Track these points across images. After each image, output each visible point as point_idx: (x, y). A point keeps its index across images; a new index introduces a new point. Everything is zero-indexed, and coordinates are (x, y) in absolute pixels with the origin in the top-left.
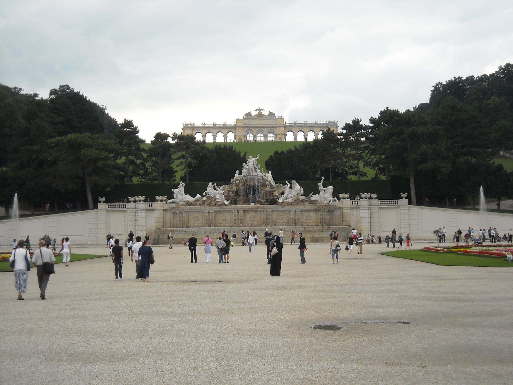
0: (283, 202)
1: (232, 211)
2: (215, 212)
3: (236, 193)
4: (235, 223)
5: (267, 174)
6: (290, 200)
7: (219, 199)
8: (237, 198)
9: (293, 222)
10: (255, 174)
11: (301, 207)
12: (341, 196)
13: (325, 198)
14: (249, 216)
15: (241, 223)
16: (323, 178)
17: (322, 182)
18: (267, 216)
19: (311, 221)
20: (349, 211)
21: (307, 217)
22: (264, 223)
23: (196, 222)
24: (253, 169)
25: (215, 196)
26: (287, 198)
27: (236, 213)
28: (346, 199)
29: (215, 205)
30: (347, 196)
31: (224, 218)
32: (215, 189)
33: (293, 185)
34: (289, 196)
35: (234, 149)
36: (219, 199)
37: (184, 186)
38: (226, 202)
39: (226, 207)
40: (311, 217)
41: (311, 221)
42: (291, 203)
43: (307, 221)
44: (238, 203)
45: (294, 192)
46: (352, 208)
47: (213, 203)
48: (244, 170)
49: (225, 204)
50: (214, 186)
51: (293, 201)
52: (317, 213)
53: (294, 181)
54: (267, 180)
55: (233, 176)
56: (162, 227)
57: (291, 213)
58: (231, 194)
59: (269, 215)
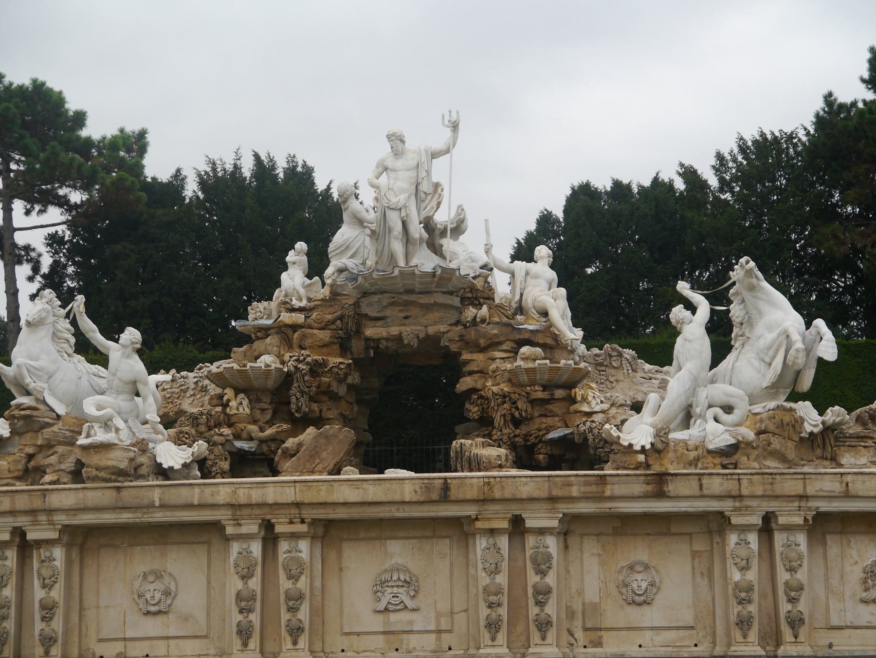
0: (657, 450)
1: (216, 527)
2: (85, 539)
3: (275, 397)
4: (245, 633)
6: (715, 433)
7: (106, 424)
9: (744, 623)
10: (425, 262)
11: (823, 483)
15: (295, 632)
18: (517, 576)
22: (493, 626)
24: (417, 230)
25: (76, 403)
26: (687, 417)
27: (256, 548)
29: (77, 475)
31: (153, 591)
32: (84, 347)
33: (736, 312)
34: (704, 395)
35: (320, 185)
36: (106, 424)
38: (172, 455)
39: (154, 491)
42: (730, 453)
45: (749, 368)
47: (59, 461)
48: (344, 234)
49: (164, 473)
50: (74, 323)
51: (749, 434)
53: (744, 269)
54: (520, 309)
55: (267, 285)
57: (733, 538)
58: (239, 406)
59: (542, 565)
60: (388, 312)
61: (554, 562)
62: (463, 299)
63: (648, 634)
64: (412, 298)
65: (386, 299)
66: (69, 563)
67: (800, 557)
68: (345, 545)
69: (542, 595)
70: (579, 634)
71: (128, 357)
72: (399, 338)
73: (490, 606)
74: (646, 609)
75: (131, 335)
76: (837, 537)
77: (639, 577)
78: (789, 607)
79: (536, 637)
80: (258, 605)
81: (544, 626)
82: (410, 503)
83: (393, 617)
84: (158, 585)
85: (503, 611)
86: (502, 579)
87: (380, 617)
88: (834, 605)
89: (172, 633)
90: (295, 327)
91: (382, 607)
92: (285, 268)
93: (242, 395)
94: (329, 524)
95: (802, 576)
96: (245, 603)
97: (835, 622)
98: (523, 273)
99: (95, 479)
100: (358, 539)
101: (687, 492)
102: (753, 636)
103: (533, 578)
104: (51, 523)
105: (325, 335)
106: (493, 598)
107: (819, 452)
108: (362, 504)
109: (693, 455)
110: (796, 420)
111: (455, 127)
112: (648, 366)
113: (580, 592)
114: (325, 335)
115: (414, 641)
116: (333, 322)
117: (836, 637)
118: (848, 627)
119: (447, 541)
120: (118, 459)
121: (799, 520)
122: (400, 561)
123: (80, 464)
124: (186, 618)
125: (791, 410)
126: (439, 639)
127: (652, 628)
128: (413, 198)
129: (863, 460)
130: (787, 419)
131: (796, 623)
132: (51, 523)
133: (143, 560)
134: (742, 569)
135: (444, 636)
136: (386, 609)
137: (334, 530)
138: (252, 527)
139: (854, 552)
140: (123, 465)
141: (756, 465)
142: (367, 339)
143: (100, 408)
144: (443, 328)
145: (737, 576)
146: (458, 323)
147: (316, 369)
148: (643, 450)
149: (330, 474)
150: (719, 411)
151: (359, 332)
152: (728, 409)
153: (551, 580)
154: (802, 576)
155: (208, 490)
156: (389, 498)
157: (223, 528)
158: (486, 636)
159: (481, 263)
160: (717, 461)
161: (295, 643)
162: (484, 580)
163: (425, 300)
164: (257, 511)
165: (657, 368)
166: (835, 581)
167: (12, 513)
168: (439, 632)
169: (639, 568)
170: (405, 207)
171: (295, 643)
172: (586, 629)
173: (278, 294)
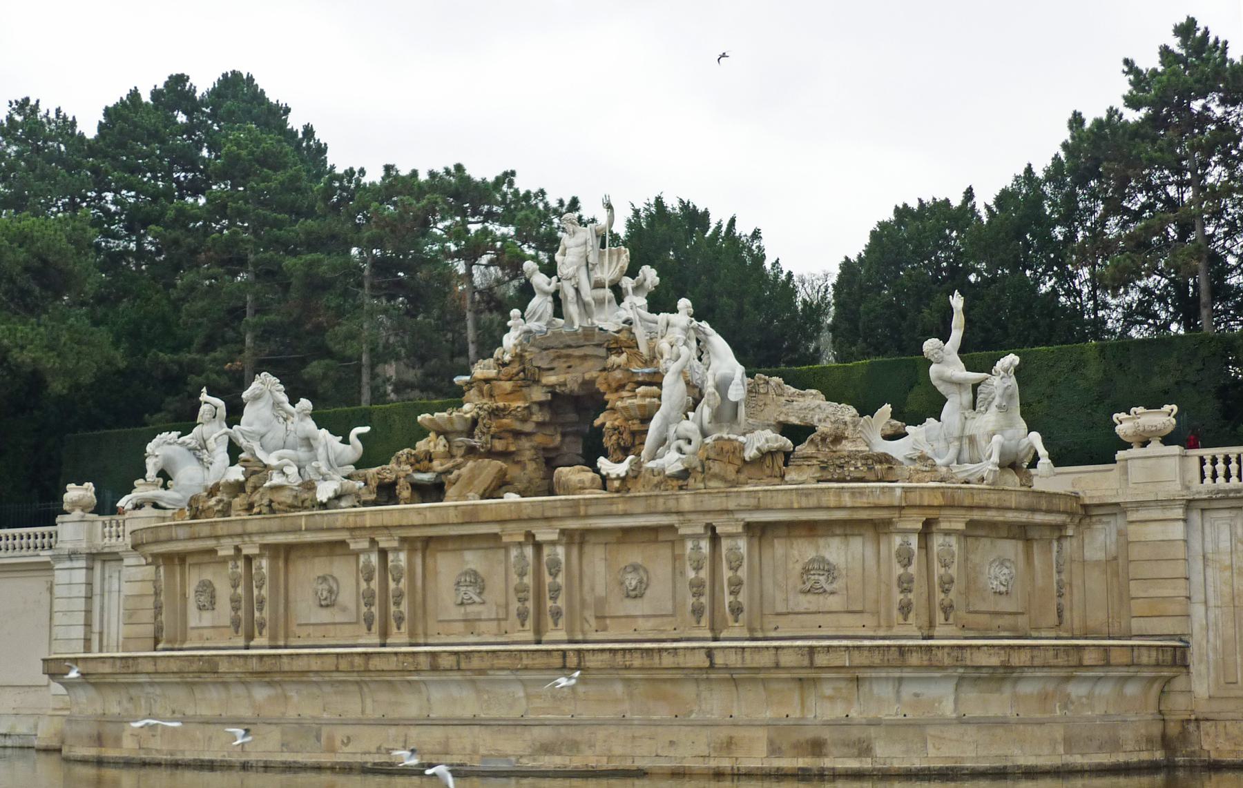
1: (343, 543)
2: (284, 553)
5: (663, 317)
6: (671, 461)
8: (449, 472)
9: (697, 612)
12: (1125, 424)
13: (972, 440)
14: (447, 568)
16: (957, 301)
17: (957, 335)
19: (834, 602)
20: (1177, 531)
21: (806, 571)
23: (207, 619)
28: (1156, 448)
30: (1164, 418)
37: (222, 411)
40: (830, 571)
41: (834, 602)
43: (805, 602)
44: (451, 491)
46: (1189, 504)
49: (323, 506)
52: (884, 540)
56: (151, 643)
57: (689, 545)
60: (555, 364)
61: (563, 566)
62: (609, 349)
63: (640, 621)
64: (570, 351)
65: (552, 353)
66: (273, 570)
67: (740, 559)
68: (440, 556)
69: (556, 591)
70: (593, 622)
71: (302, 420)
72: (564, 384)
73: (519, 600)
74: (638, 601)
75: (305, 403)
76: (783, 541)
77: (629, 576)
78: (732, 598)
79: (551, 624)
80: (377, 601)
81: (557, 614)
82: (453, 524)
83: (470, 609)
84: (325, 586)
85: (530, 605)
86: (528, 580)
87: (462, 609)
88: (779, 596)
89: (337, 620)
90: (487, 381)
91: (459, 601)
92: (507, 330)
93: (441, 437)
94: (428, 541)
95: (743, 573)
96: (369, 599)
97: (780, 608)
98: (664, 324)
99: (280, 511)
100: (447, 551)
101: (640, 510)
102: (705, 621)
103: (548, 579)
104: (253, 543)
105: (508, 386)
106: (521, 595)
107: (768, 471)
108: (425, 525)
109: (656, 479)
110: (735, 448)
111: (609, 207)
112: (793, 390)
113: (593, 589)
114: (508, 386)
115: (483, 626)
116: (517, 374)
117: (782, 621)
118: (789, 613)
119: (503, 551)
120: (285, 497)
121: (740, 530)
122: (472, 566)
123: (271, 501)
124: (344, 609)
125: (729, 439)
126: (499, 625)
127: (643, 616)
128: (583, 271)
129: (804, 477)
130: (727, 447)
131: (736, 610)
132: (253, 543)
133: (320, 566)
134: (697, 569)
135: (503, 623)
136: (462, 604)
137: (426, 544)
138: (365, 544)
139: (796, 553)
140: (289, 501)
141: (702, 485)
142: (545, 386)
143: (280, 458)
144: (594, 374)
145: (691, 574)
146: (604, 369)
147: (495, 413)
148: (618, 477)
149: (483, 497)
150: (682, 443)
151: (537, 382)
152: (690, 442)
153: (561, 579)
154: (743, 573)
155: (331, 518)
156: (440, 521)
157: (348, 545)
158: (518, 623)
159: (624, 318)
160: (675, 483)
161: (399, 628)
162: (515, 579)
163: (577, 352)
164: (364, 533)
165: (798, 391)
166: (780, 577)
167: (230, 536)
168: (499, 620)
169: (629, 570)
170: (574, 276)
171: (399, 628)
172: (597, 617)
173: (498, 352)
